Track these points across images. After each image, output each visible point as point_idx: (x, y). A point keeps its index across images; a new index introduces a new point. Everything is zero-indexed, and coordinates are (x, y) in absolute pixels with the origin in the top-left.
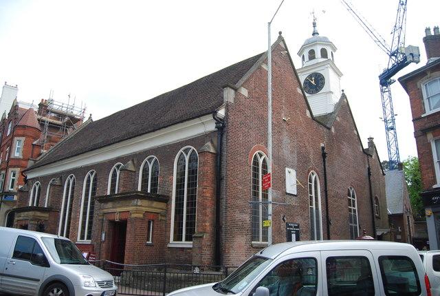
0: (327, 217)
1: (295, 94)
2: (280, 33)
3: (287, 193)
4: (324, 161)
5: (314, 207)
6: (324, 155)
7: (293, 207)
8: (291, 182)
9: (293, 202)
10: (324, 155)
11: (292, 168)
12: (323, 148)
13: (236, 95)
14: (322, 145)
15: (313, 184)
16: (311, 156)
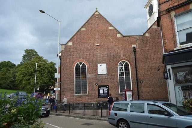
0: (137, 80)
1: (107, 30)
2: (97, 9)
3: (98, 74)
4: (135, 54)
5: (124, 76)
6: (135, 51)
7: (104, 79)
8: (102, 69)
9: (104, 77)
10: (135, 51)
11: (102, 63)
12: (134, 47)
13: (65, 46)
14: (133, 46)
15: (124, 67)
16: (121, 55)
